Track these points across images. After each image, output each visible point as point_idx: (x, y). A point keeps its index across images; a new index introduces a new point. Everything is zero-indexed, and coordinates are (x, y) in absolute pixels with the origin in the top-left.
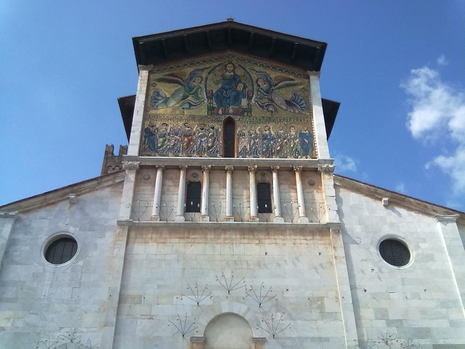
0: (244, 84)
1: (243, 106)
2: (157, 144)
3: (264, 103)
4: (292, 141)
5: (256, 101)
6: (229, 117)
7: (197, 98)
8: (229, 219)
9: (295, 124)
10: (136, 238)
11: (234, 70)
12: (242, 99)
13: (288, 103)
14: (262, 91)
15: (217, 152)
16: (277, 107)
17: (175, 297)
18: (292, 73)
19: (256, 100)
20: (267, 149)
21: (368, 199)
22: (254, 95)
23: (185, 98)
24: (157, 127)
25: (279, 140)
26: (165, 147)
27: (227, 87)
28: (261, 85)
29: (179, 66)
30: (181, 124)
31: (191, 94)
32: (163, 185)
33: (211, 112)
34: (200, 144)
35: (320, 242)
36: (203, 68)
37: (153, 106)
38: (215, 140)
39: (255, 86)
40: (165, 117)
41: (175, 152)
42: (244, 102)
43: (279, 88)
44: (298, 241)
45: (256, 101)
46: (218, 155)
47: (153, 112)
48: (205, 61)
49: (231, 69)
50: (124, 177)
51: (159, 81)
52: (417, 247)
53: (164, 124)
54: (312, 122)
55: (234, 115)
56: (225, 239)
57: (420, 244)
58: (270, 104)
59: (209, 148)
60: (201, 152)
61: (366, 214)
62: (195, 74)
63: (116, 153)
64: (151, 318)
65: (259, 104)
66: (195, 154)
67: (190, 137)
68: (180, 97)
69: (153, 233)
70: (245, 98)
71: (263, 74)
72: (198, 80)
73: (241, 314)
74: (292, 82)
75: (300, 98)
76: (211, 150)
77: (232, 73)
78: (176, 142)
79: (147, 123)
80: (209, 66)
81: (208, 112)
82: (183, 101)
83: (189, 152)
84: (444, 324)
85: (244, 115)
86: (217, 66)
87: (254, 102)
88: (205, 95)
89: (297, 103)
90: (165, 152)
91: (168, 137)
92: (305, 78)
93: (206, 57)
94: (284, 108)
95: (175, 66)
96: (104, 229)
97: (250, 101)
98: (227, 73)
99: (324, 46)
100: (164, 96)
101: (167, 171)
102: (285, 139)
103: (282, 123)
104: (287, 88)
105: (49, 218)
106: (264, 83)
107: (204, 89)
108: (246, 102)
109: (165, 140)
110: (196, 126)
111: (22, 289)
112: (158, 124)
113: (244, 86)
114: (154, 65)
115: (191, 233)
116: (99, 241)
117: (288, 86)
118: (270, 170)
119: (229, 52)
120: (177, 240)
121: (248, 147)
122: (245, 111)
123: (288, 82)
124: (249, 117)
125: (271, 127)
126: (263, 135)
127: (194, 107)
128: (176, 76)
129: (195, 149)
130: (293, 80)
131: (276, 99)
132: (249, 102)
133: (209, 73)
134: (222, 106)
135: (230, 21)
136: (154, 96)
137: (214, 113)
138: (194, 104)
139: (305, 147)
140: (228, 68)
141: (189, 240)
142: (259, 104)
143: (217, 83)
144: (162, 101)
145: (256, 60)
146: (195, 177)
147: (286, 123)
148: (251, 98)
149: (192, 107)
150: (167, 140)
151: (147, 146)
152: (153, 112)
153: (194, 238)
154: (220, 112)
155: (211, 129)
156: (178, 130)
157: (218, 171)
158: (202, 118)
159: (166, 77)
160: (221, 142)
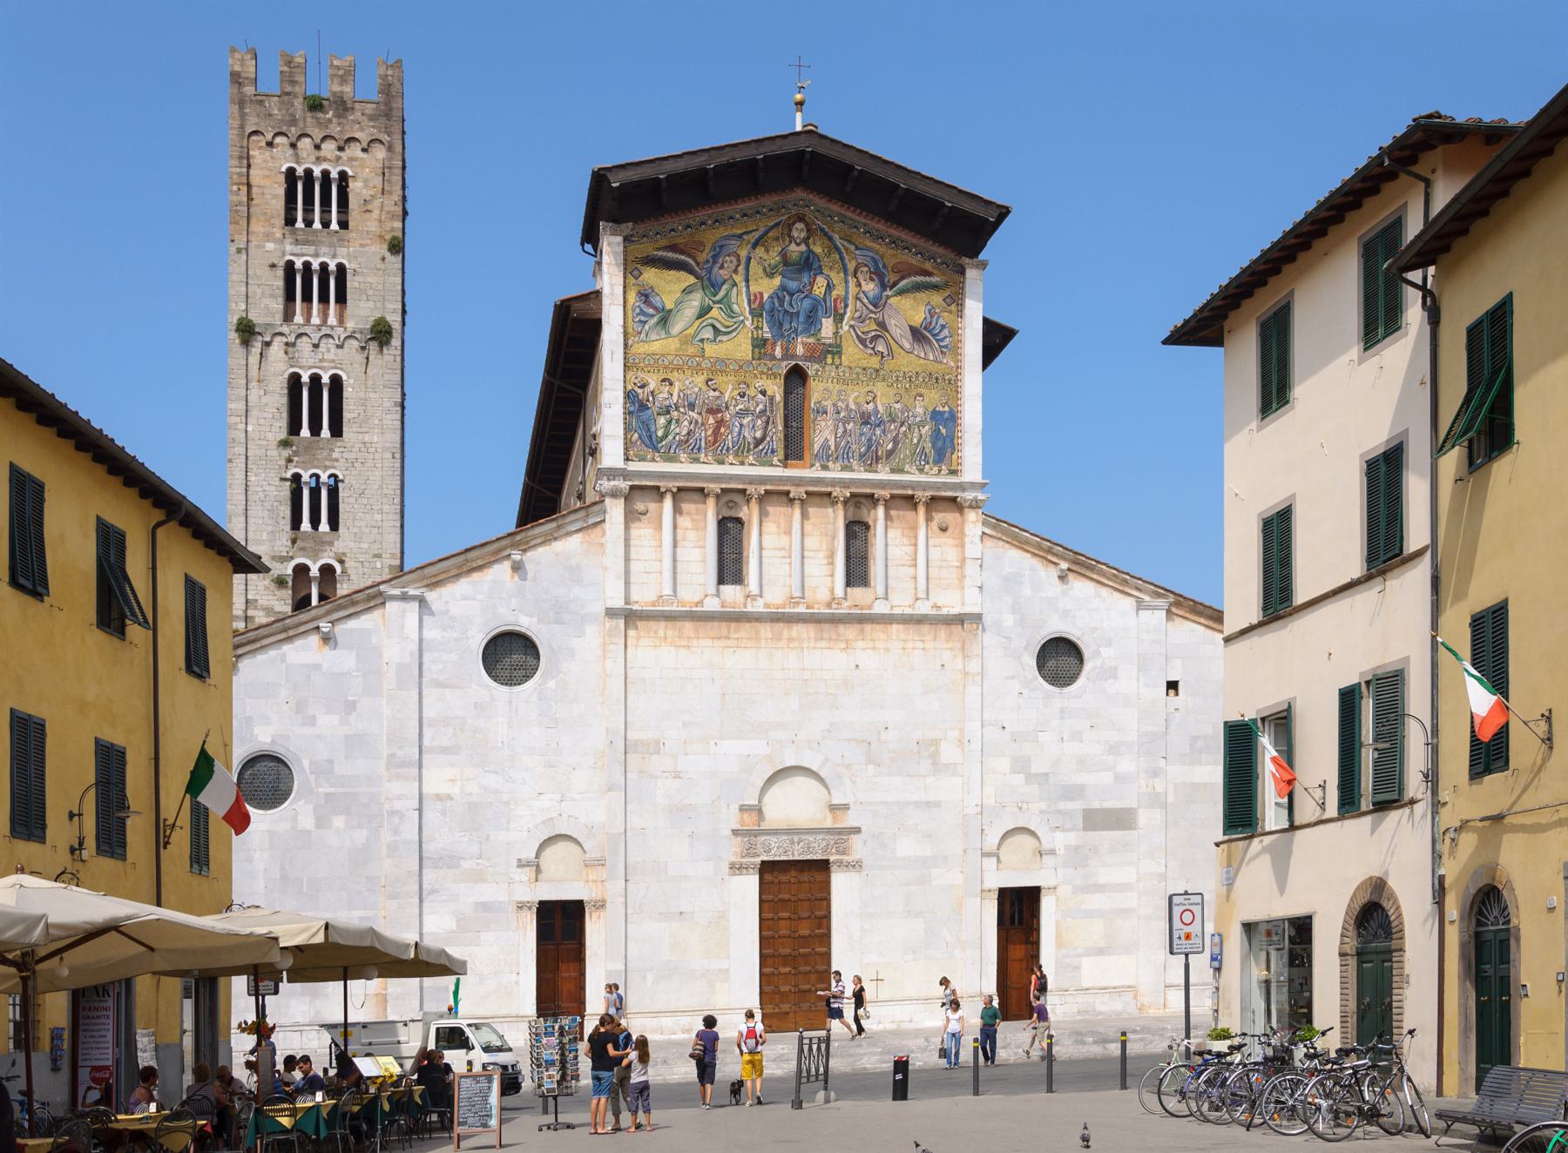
0: (828, 278)
1: (825, 338)
2: (656, 432)
3: (868, 332)
4: (916, 430)
5: (852, 326)
6: (797, 365)
7: (731, 314)
8: (798, 603)
9: (926, 387)
11: (808, 238)
12: (823, 320)
13: (917, 334)
15: (773, 452)
17: (712, 743)
18: (932, 258)
19: (852, 323)
20: (869, 447)
22: (848, 310)
23: (704, 312)
24: (652, 386)
25: (892, 427)
26: (670, 437)
27: (793, 285)
29: (688, 226)
31: (719, 302)
32: (675, 527)
33: (760, 353)
34: (739, 434)
36: (739, 232)
37: (640, 333)
38: (767, 422)
39: (850, 285)
40: (666, 363)
41: (692, 450)
42: (827, 327)
43: (901, 293)
45: (852, 326)
46: (775, 459)
47: (639, 349)
48: (745, 215)
49: (803, 235)
50: (605, 512)
51: (646, 264)
53: (664, 380)
54: (959, 384)
55: (806, 361)
56: (790, 640)
58: (878, 337)
59: (758, 442)
60: (743, 452)
62: (721, 247)
64: (677, 777)
65: (858, 336)
66: (731, 457)
67: (720, 415)
68: (693, 310)
70: (829, 317)
71: (871, 254)
72: (730, 262)
74: (928, 279)
75: (941, 322)
76: (761, 447)
77: (803, 248)
78: (692, 427)
80: (754, 228)
81: (753, 352)
82: (700, 320)
83: (719, 452)
85: (826, 363)
87: (846, 328)
88: (746, 305)
89: (933, 335)
90: (672, 451)
91: (676, 413)
92: (957, 272)
93: (748, 205)
94: (907, 346)
95: (680, 224)
97: (839, 325)
98: (793, 247)
99: (1004, 212)
100: (659, 305)
101: (678, 496)
102: (901, 426)
103: (900, 386)
104: (918, 295)
105: (480, 597)
106: (872, 279)
107: (744, 289)
108: (831, 328)
109: (670, 422)
110: (730, 387)
113: (828, 284)
114: (635, 222)
115: (732, 629)
117: (918, 288)
118: (872, 499)
119: (800, 194)
120: (709, 642)
121: (832, 443)
122: (828, 352)
123: (919, 279)
124: (837, 368)
125: (879, 394)
126: (863, 415)
127: (724, 338)
128: (682, 252)
129: (730, 446)
130: (929, 274)
131: (893, 322)
132: (837, 327)
133: (754, 246)
134: (782, 335)
135: (811, 131)
136: (637, 304)
137: (765, 354)
138: (723, 330)
140: (795, 234)
141: (729, 643)
143: (771, 275)
144: (655, 319)
145: (858, 218)
146: (731, 508)
147: (907, 386)
148: (842, 319)
149: (719, 338)
150: (674, 421)
151: (636, 435)
153: (737, 639)
154: (778, 352)
155: (760, 396)
156: (694, 396)
157: (775, 498)
159: (660, 253)
160: (780, 428)
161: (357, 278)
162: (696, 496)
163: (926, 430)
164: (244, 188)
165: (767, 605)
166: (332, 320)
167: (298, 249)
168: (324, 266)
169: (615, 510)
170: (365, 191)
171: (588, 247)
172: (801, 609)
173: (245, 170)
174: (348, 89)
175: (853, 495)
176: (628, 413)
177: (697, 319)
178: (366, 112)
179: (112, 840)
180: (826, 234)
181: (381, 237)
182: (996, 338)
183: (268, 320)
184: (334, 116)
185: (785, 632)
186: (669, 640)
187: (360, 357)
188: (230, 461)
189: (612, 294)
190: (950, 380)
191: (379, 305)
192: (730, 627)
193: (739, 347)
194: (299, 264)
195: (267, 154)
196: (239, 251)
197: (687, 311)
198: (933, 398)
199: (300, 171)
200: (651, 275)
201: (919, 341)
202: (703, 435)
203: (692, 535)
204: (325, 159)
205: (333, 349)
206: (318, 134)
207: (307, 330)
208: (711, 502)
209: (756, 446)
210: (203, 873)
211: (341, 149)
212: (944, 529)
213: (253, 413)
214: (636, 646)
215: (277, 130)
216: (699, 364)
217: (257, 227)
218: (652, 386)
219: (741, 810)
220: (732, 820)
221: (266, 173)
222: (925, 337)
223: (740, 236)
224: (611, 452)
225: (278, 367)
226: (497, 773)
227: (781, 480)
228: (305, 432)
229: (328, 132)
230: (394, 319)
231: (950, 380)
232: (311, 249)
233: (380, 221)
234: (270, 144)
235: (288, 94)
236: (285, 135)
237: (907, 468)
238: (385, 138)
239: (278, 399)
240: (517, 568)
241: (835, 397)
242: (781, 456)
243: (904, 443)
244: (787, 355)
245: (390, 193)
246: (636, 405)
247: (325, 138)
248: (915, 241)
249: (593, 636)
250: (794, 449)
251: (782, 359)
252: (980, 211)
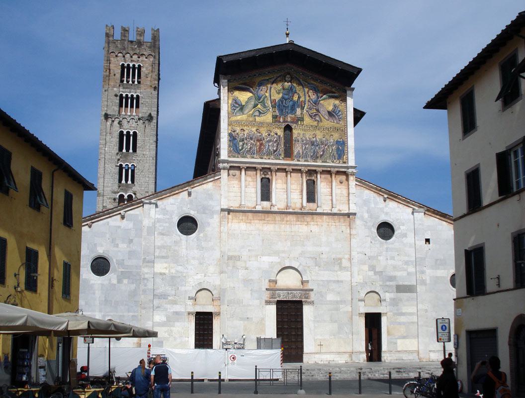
0: (298, 94)
7: (265, 107)
8: (289, 208)
10: (232, 219)
13: (330, 114)
14: (312, 102)
15: (280, 155)
16: (321, 117)
18: (335, 87)
21: (375, 195)
22: (306, 105)
23: (255, 106)
24: (237, 132)
26: (244, 149)
27: (286, 97)
28: (311, 96)
29: (249, 77)
30: (254, 129)
31: (261, 102)
32: (246, 181)
34: (268, 148)
35: (343, 224)
38: (278, 144)
42: (299, 111)
44: (330, 224)
47: (234, 118)
52: (400, 228)
53: (241, 130)
56: (287, 221)
57: (401, 227)
59: (275, 151)
61: (373, 206)
63: (118, 36)
64: (246, 269)
65: (309, 114)
69: (242, 216)
73: (296, 267)
75: (338, 109)
77: (290, 84)
79: (230, 127)
84: (404, 274)
86: (278, 77)
87: (305, 112)
94: (327, 118)
96: (213, 213)
98: (286, 83)
100: (240, 103)
106: (314, 94)
109: (244, 144)
111: (170, 251)
112: (238, 129)
116: (211, 221)
118: (315, 172)
121: (301, 152)
122: (299, 120)
127: (263, 115)
130: (334, 93)
131: (322, 109)
133: (272, 84)
137: (277, 121)
139: (339, 152)
140: (287, 79)
141: (265, 222)
142: (309, 114)
143: (279, 93)
144: (239, 108)
145: (308, 73)
152: (234, 118)
154: (281, 120)
158: (268, 124)
159: (240, 86)
161: (143, 100)
162: (253, 170)
163: (334, 147)
164: (108, 70)
165: (278, 209)
166: (134, 114)
167: (124, 90)
168: (132, 96)
169: (224, 174)
171: (216, 84)
172: (291, 210)
174: (142, 38)
175: (309, 170)
176: (230, 141)
177: (254, 107)
178: (148, 45)
179: (31, 285)
180: (298, 79)
181: (151, 86)
182: (359, 115)
183: (114, 113)
184: (137, 47)
185: (285, 218)
186: (244, 220)
187: (143, 126)
188: (100, 160)
189: (224, 100)
190: (342, 130)
192: (265, 216)
193: (268, 118)
194: (124, 95)
196: (105, 91)
197: (249, 106)
198: (336, 136)
199: (126, 65)
200: (237, 93)
201: (331, 116)
202: (255, 149)
203: (252, 184)
204: (134, 61)
205: (134, 123)
206: (132, 53)
207: (126, 117)
208: (258, 172)
209: (274, 153)
210: (67, 298)
211: (139, 57)
212: (341, 183)
213: (108, 144)
214: (232, 222)
216: (254, 124)
217: (112, 83)
218: (237, 132)
219: (269, 281)
220: (266, 284)
221: (115, 65)
222: (333, 115)
223: (268, 80)
224: (224, 154)
225: (116, 129)
226: (182, 266)
227: (283, 164)
228: (124, 150)
229: (135, 52)
230: (154, 114)
231: (342, 130)
232: (129, 90)
233: (151, 81)
234: (116, 56)
235: (123, 40)
236: (121, 53)
237: (328, 161)
238: (153, 54)
239: (116, 140)
240: (190, 194)
241: (301, 136)
242: (283, 157)
243: (327, 152)
244: (284, 121)
245: (154, 72)
246: (232, 138)
247: (134, 54)
248: (329, 81)
249: (216, 218)
250: (288, 154)
251: (283, 122)
252: (351, 70)
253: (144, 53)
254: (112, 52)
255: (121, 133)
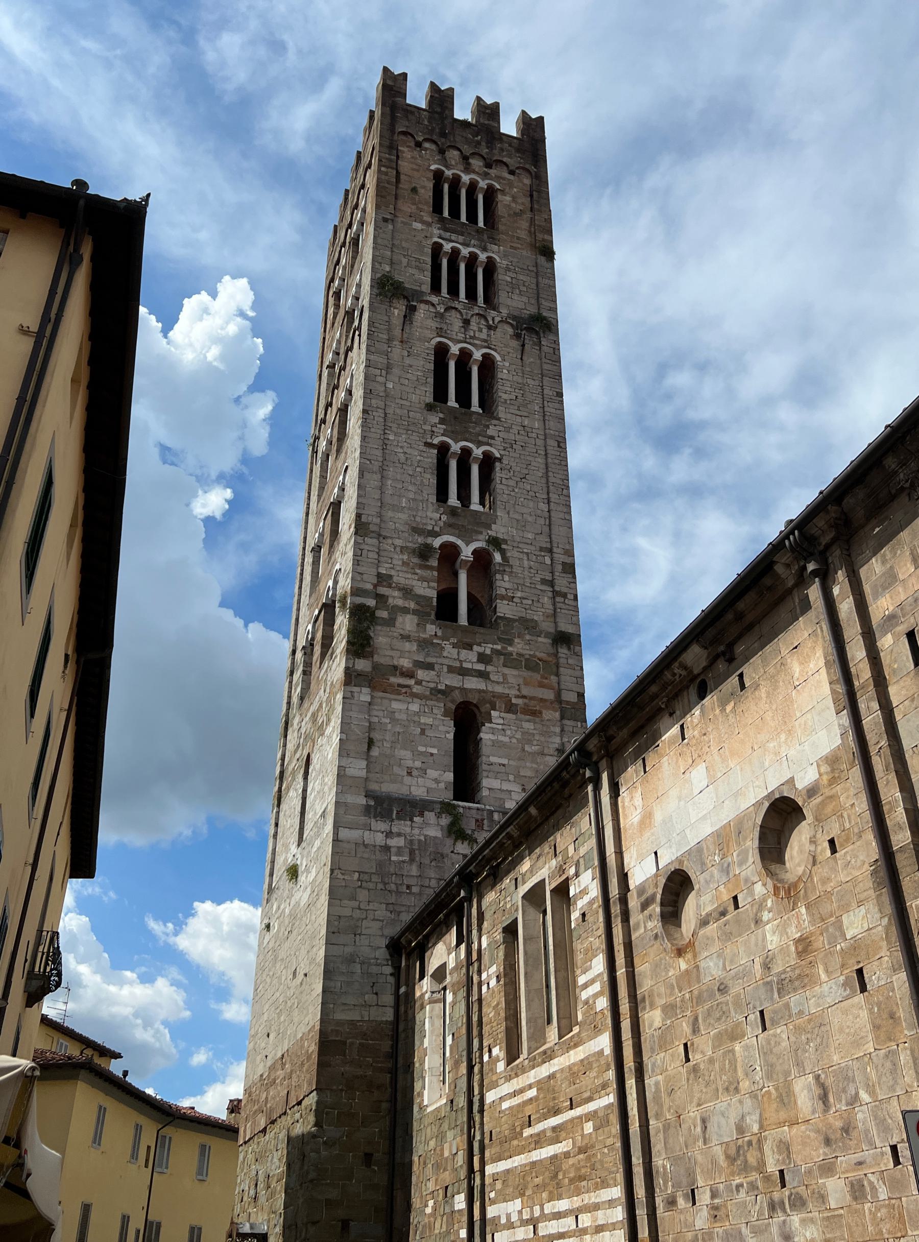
170: (513, 205)
173: (394, 158)
187: (515, 344)
191: (533, 301)
195: (415, 153)
204: (474, 172)
205: (485, 331)
211: (489, 166)
215: (427, 136)
221: (415, 167)
232: (461, 239)
234: (419, 145)
253: (505, 160)
254: (404, 133)
255: (441, 352)
